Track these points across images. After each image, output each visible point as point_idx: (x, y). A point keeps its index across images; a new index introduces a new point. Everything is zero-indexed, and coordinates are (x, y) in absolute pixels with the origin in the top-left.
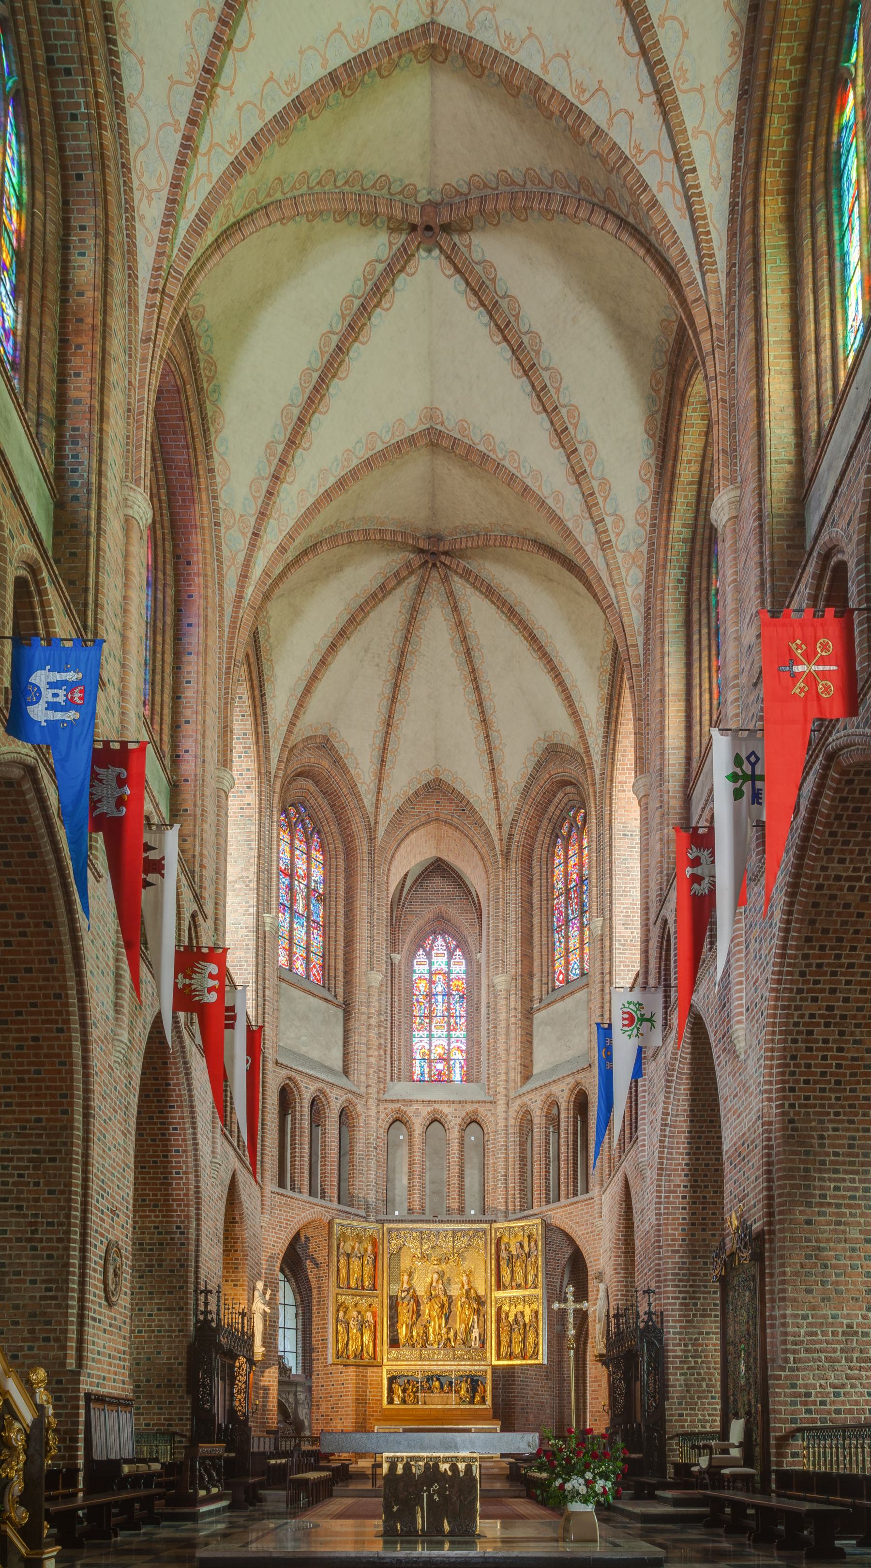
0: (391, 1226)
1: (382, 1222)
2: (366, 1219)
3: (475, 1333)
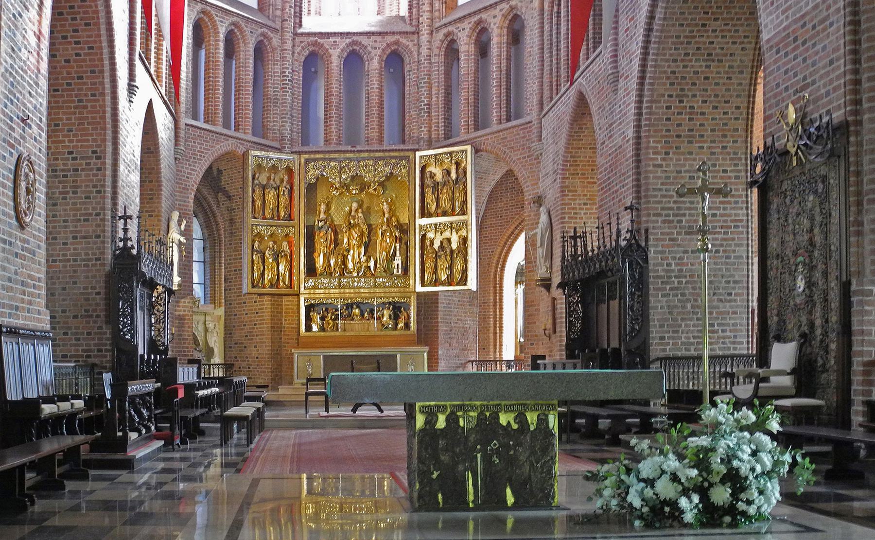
0: (307, 156)
1: (299, 153)
2: (280, 150)
3: (398, 261)
